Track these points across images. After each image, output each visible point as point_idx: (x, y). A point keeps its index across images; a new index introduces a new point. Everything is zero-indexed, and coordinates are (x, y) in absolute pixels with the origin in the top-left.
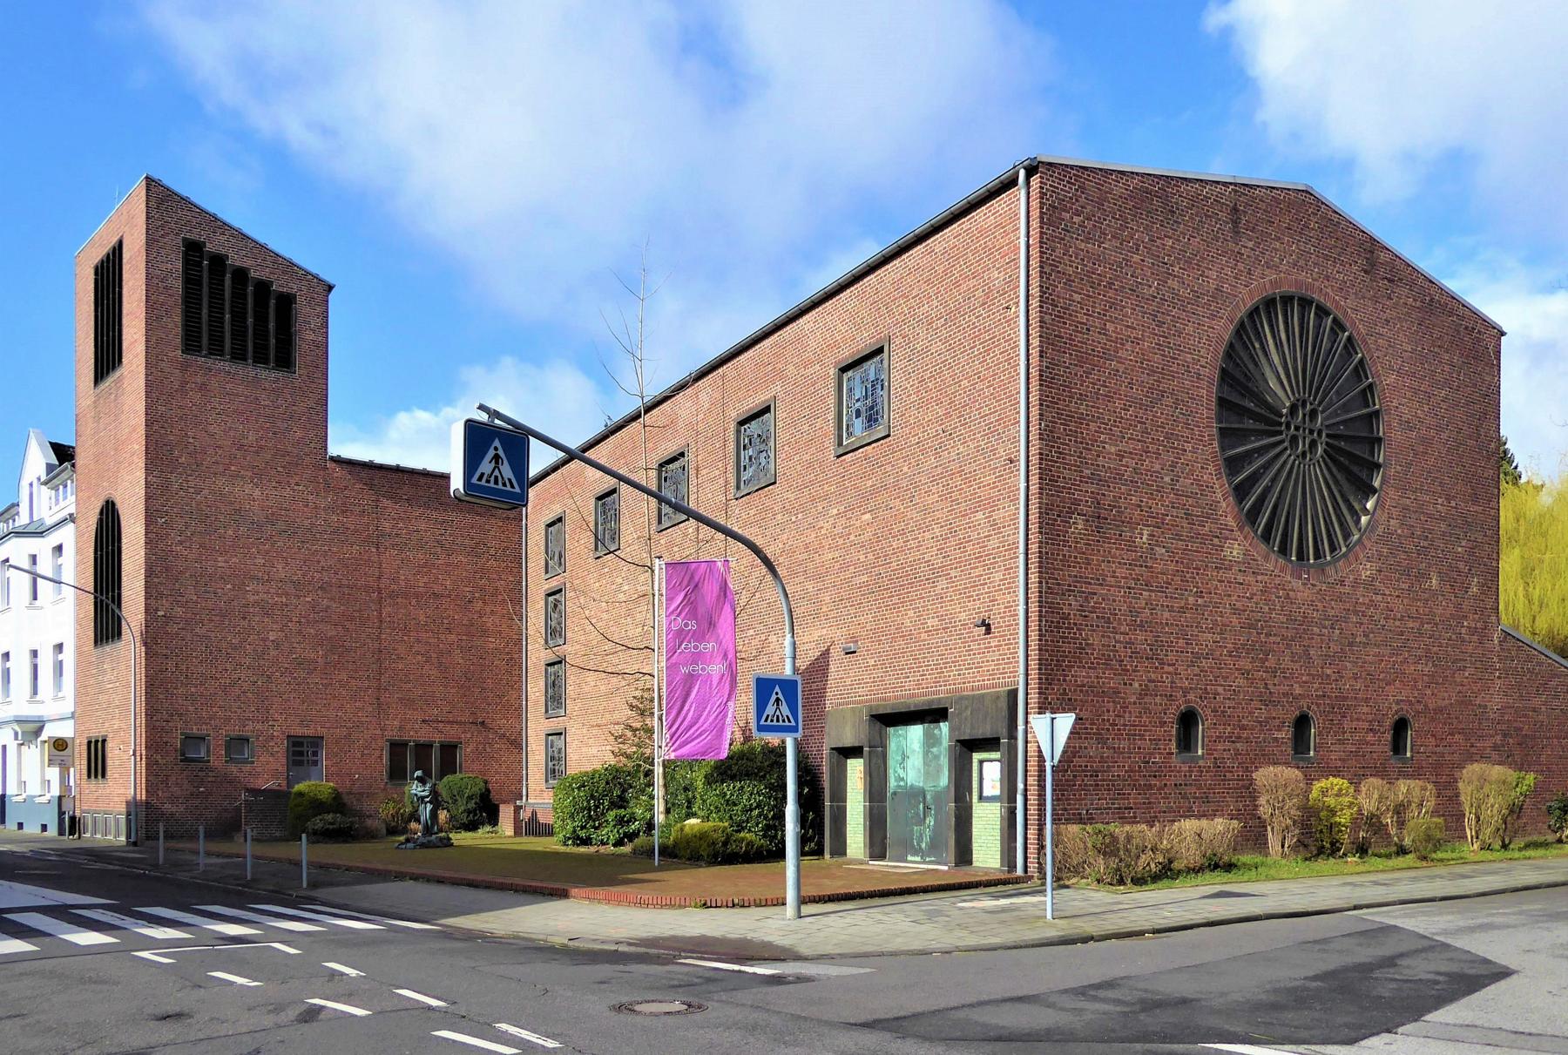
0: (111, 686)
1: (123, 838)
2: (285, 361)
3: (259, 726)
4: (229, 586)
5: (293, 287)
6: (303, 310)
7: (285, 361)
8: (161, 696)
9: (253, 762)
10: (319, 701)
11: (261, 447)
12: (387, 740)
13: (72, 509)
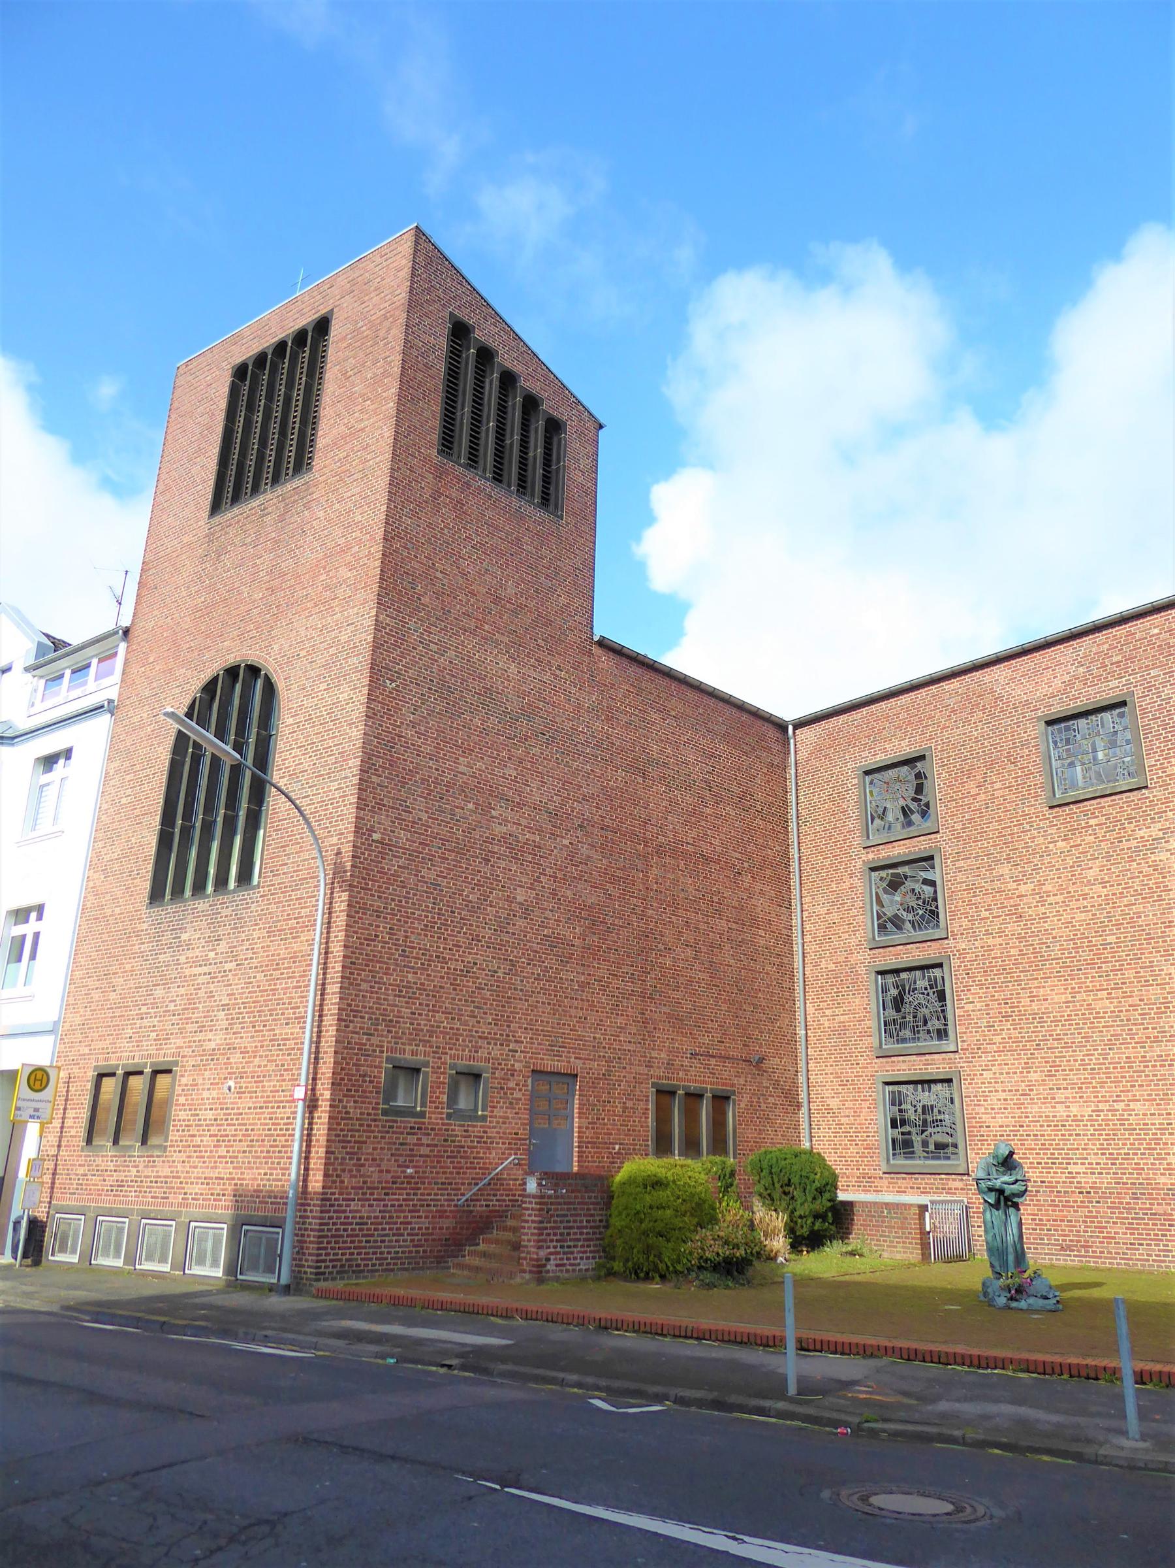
0: (205, 969)
1: (219, 1273)
2: (548, 498)
3: (496, 1052)
4: (471, 806)
5: (562, 414)
6: (572, 443)
7: (548, 498)
8: (364, 986)
9: (484, 1118)
10: (573, 1012)
11: (520, 606)
12: (653, 1085)
13: (113, 694)
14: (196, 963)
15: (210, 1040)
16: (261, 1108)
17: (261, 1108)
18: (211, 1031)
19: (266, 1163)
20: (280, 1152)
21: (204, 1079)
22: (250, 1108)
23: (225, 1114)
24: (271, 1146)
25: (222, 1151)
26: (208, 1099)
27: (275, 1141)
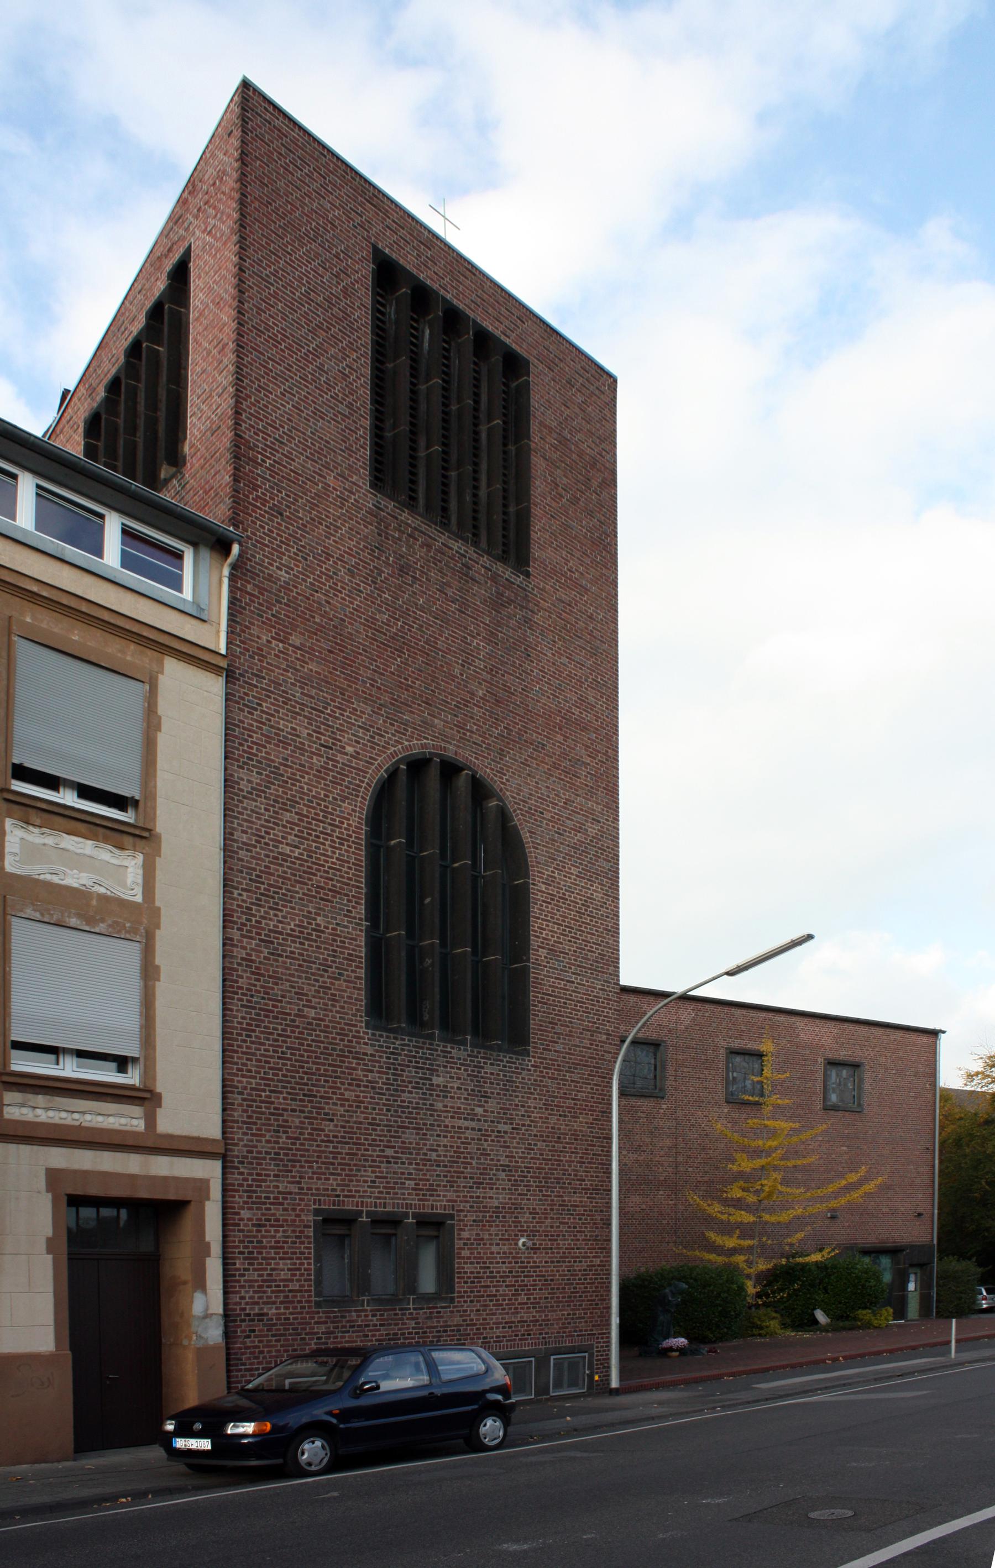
14: (456, 1114)
15: (491, 1198)
16: (558, 1262)
17: (558, 1262)
18: (492, 1189)
19: (569, 1306)
20: (580, 1296)
21: (490, 1235)
22: (546, 1262)
23: (520, 1267)
24: (572, 1293)
25: (523, 1298)
26: (499, 1253)
27: (575, 1288)
